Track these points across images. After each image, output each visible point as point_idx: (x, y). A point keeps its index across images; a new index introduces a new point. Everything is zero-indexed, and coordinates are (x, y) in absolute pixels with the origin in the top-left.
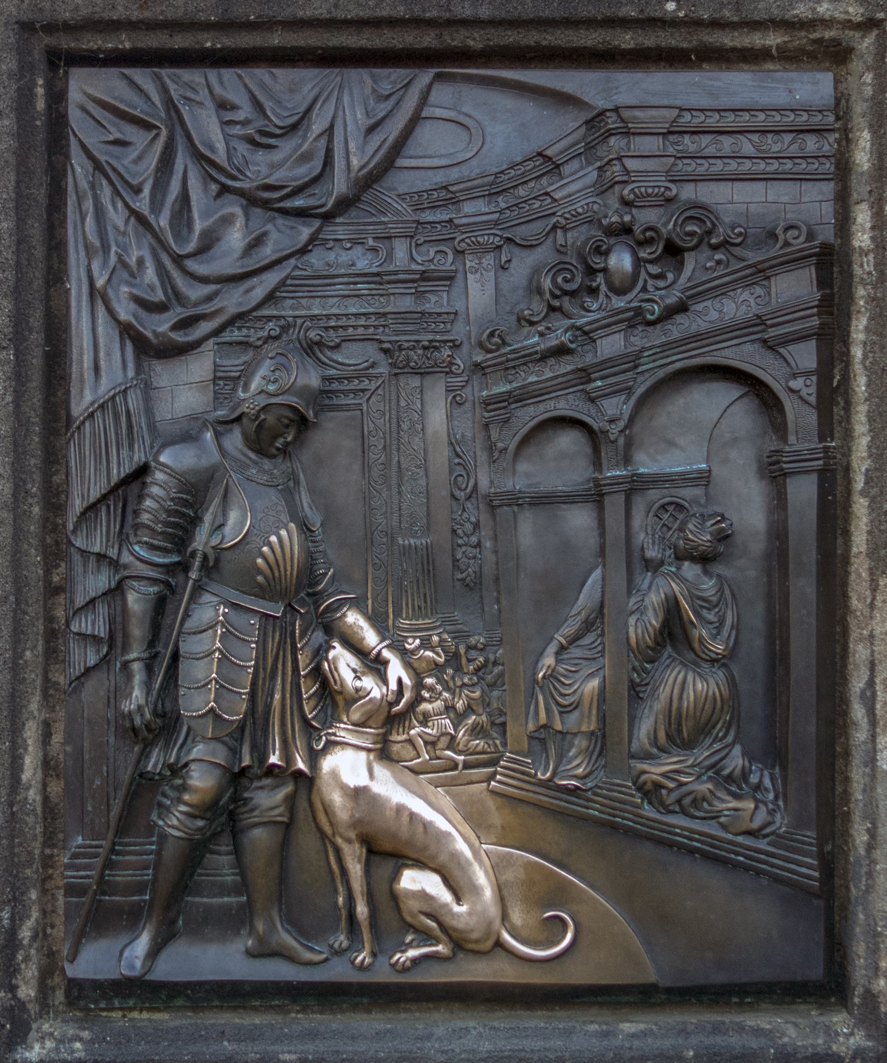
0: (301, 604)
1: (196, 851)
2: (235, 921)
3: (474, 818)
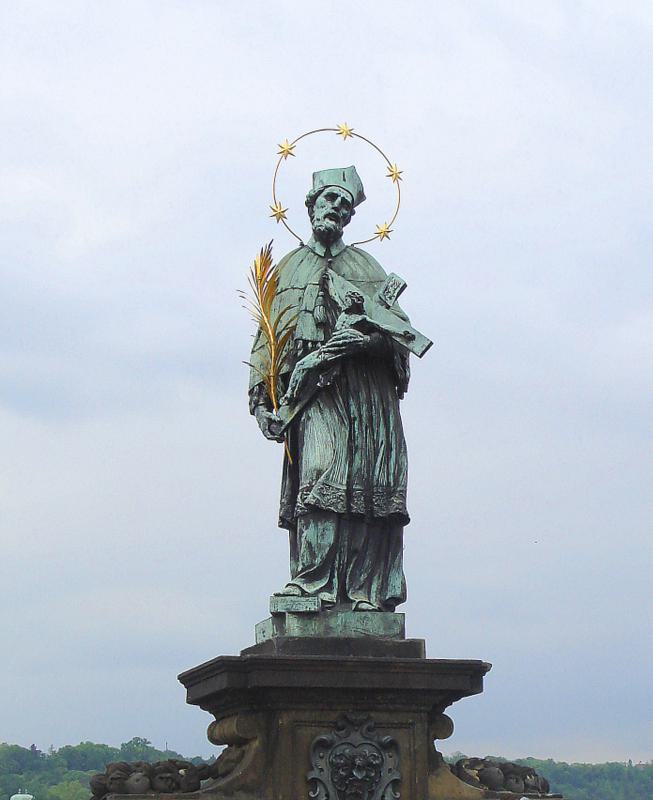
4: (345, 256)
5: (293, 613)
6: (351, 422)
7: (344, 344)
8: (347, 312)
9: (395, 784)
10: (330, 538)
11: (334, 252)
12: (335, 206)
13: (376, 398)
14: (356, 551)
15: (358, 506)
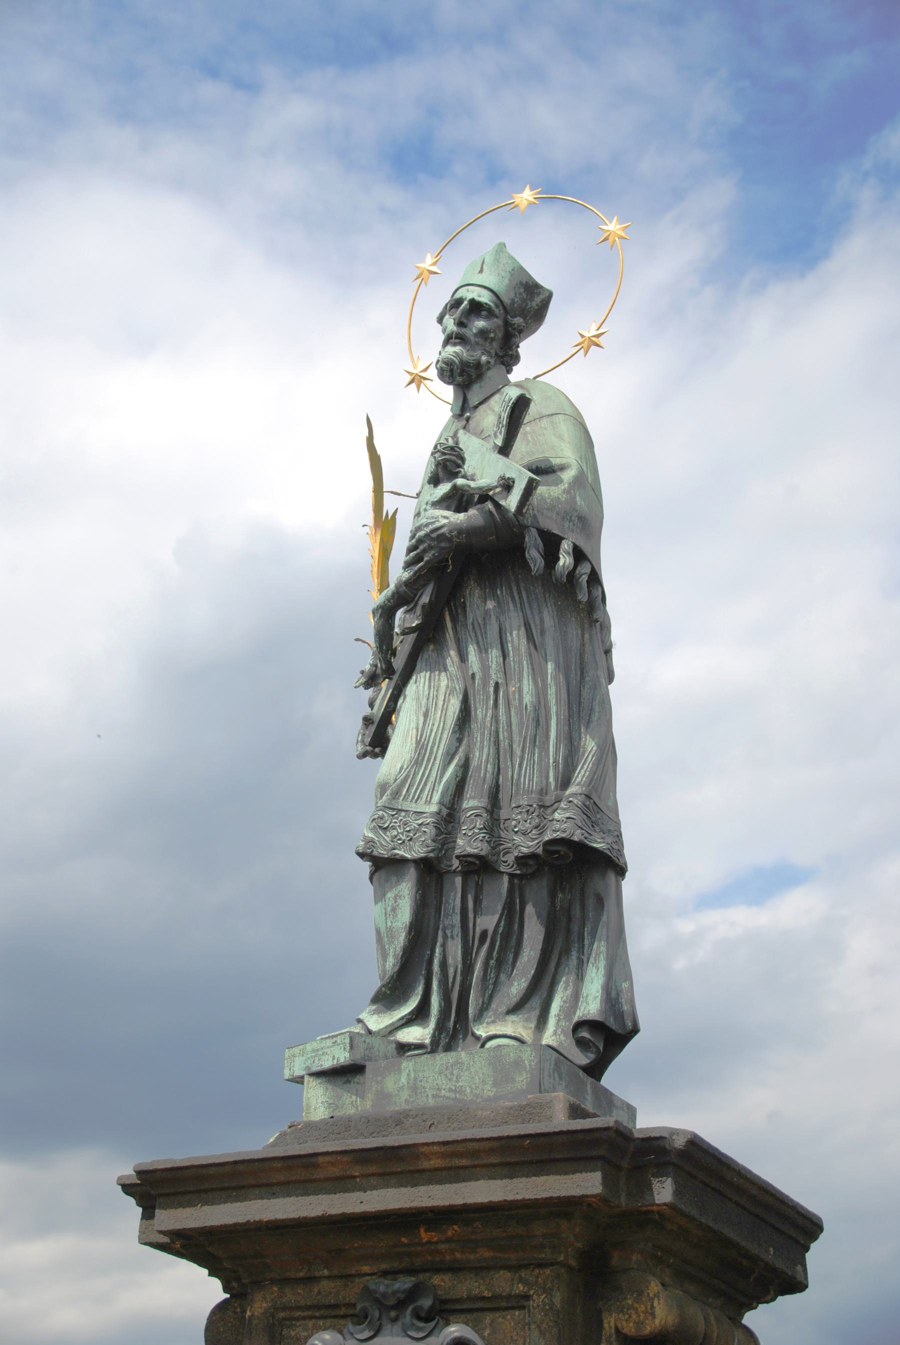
7: (420, 541)
10: (405, 915)
11: (474, 397)
15: (469, 842)
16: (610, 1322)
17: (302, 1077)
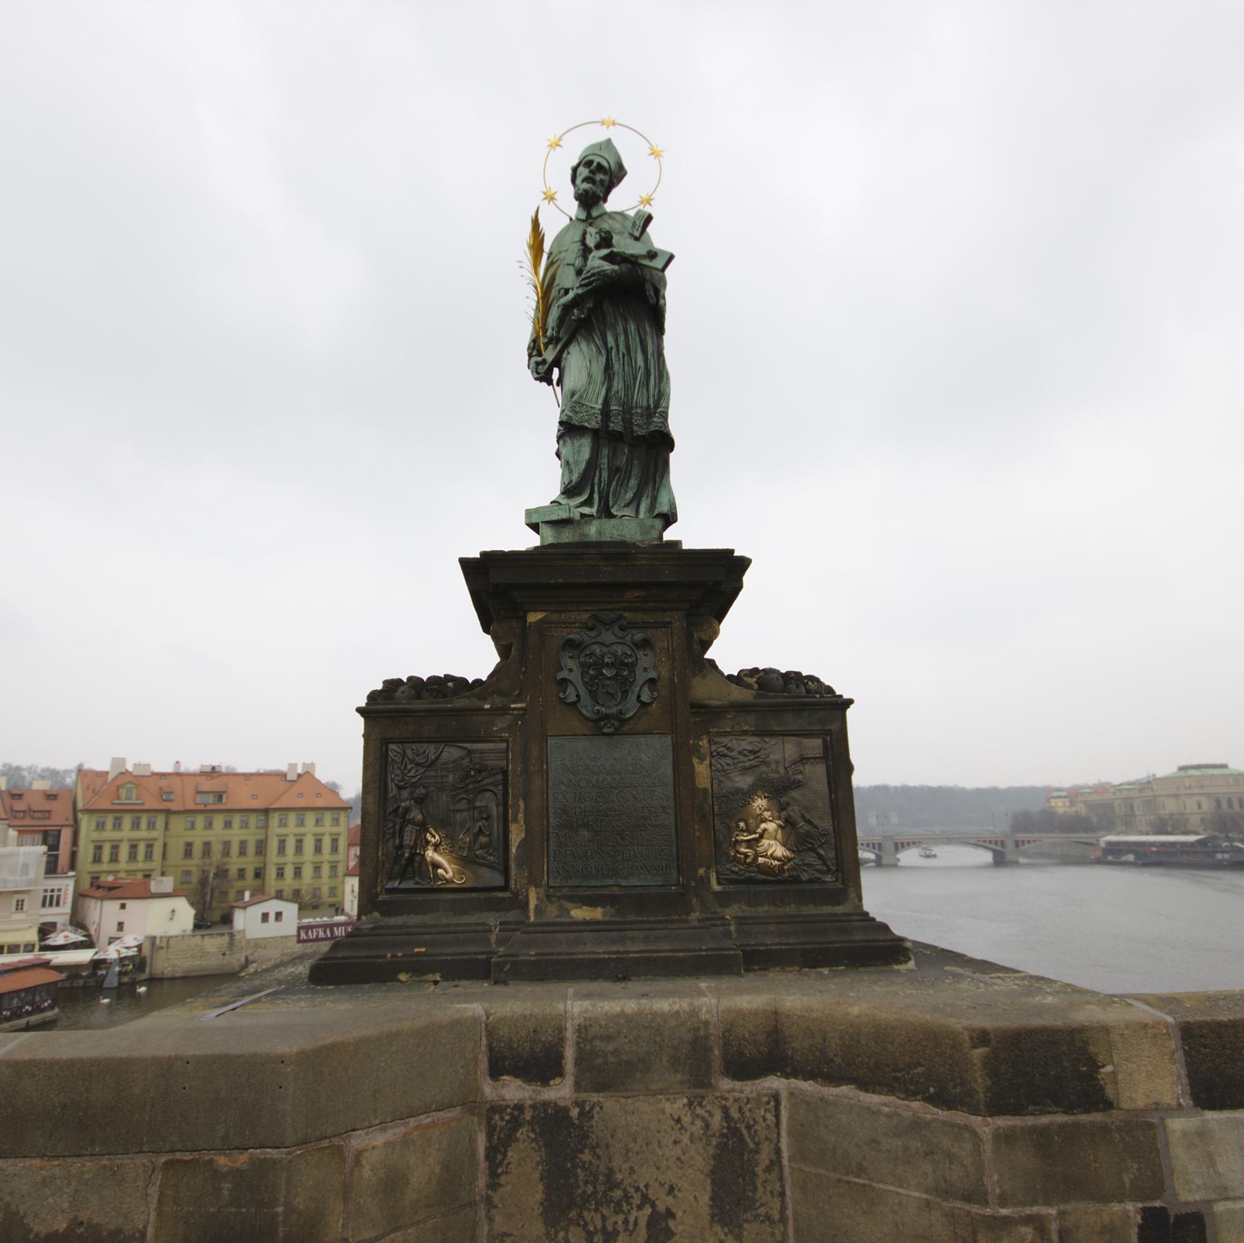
0: (423, 828)
1: (406, 866)
2: (413, 878)
3: (449, 862)
4: (605, 217)
5: (547, 522)
6: (608, 352)
7: (593, 275)
8: (598, 247)
9: (652, 682)
10: (586, 454)
11: (595, 213)
12: (598, 176)
13: (632, 327)
14: (618, 470)
15: (616, 425)
16: (696, 636)
17: (537, 524)
